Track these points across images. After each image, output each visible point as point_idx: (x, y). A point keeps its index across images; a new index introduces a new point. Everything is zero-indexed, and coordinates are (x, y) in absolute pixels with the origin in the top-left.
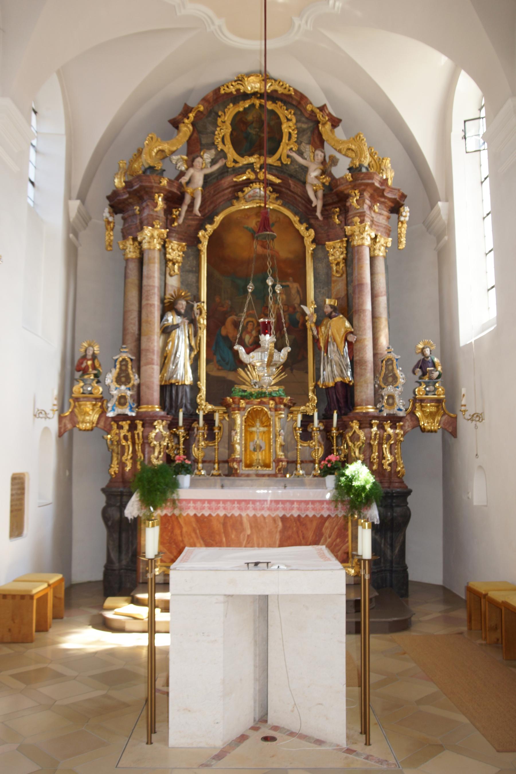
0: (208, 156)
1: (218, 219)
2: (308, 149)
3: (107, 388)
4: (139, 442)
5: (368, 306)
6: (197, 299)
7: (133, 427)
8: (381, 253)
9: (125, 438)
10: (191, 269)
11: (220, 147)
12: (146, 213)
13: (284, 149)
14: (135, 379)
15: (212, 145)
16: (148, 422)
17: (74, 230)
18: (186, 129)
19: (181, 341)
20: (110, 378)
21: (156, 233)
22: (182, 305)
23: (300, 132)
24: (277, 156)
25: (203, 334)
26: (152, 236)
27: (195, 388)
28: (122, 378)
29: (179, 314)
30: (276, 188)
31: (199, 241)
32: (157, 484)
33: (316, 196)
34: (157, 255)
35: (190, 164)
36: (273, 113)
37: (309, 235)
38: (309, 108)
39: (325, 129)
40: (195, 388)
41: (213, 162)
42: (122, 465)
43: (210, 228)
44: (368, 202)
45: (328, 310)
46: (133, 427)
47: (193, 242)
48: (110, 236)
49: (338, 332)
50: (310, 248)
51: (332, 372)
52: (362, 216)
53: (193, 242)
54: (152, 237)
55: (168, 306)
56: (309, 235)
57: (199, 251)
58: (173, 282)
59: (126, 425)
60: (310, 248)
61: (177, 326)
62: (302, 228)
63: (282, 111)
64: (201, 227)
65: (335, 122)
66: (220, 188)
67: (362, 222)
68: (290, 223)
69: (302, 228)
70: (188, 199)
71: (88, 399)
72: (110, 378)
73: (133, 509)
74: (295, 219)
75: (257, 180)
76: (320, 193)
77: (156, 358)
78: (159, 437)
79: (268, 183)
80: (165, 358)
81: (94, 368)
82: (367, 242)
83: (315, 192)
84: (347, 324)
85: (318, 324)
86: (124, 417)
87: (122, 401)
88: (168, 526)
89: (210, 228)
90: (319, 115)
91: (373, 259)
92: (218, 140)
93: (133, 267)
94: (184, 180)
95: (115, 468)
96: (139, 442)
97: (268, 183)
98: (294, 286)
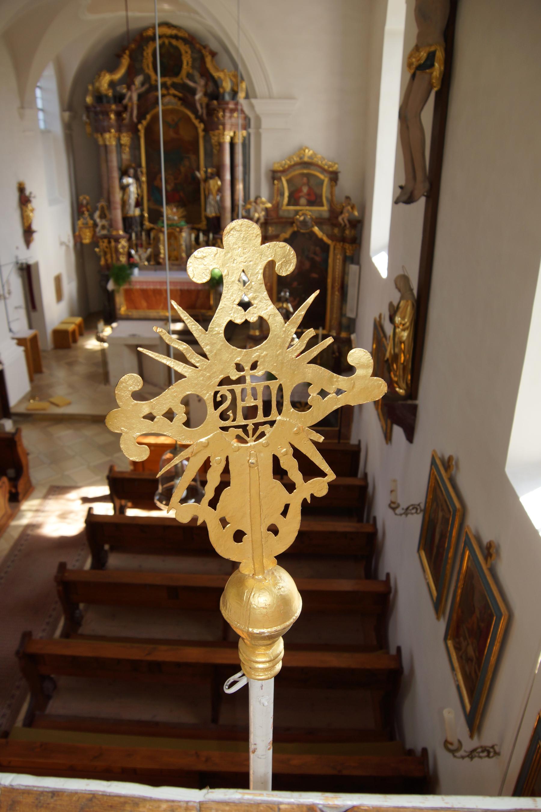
0: (139, 80)
1: (148, 117)
2: (197, 75)
3: (95, 221)
4: (113, 249)
5: (228, 177)
6: (140, 166)
7: (109, 242)
8: (239, 141)
9: (107, 247)
10: (135, 147)
11: (147, 71)
12: (106, 124)
13: (184, 73)
14: (109, 216)
15: (141, 71)
16: (117, 240)
17: (68, 127)
18: (125, 61)
19: (133, 189)
20: (97, 214)
21: (112, 135)
22: (132, 171)
23: (194, 60)
24: (179, 77)
25: (145, 186)
26: (110, 138)
27: (142, 216)
28: (103, 216)
29: (129, 176)
30: (180, 99)
31: (138, 131)
32: (122, 274)
33: (202, 108)
34: (114, 149)
35: (129, 88)
36: (177, 49)
37: (201, 126)
38: (198, 46)
39: (208, 59)
40: (142, 216)
41: (143, 84)
42: (106, 260)
43: (145, 123)
44: (228, 114)
45: (209, 175)
46: (109, 242)
47: (134, 131)
48: (89, 129)
49: (214, 186)
50: (201, 134)
51: (211, 212)
52: (224, 125)
53: (134, 131)
54: (110, 138)
55: (124, 173)
56: (201, 126)
57: (139, 138)
58: (126, 156)
59: (106, 241)
60: (201, 134)
61: (128, 185)
62: (196, 122)
63: (183, 48)
64: (139, 122)
65: (213, 54)
66: (147, 102)
67: (224, 129)
68: (189, 119)
69: (196, 122)
70: (129, 109)
71: (86, 228)
72: (97, 214)
73: (111, 286)
74: (192, 116)
75: (169, 94)
76: (204, 105)
77: (119, 206)
78: (123, 247)
79: (175, 96)
80: (124, 203)
81: (88, 211)
82: (227, 139)
83: (201, 105)
84: (219, 183)
85: (206, 180)
86: (105, 237)
87: (103, 227)
88: (128, 293)
89: (145, 123)
90: (204, 51)
91: (232, 145)
92: (145, 67)
93: (102, 150)
94: (125, 101)
95: (103, 262)
96: (113, 249)
97: (175, 96)
98: (193, 157)
